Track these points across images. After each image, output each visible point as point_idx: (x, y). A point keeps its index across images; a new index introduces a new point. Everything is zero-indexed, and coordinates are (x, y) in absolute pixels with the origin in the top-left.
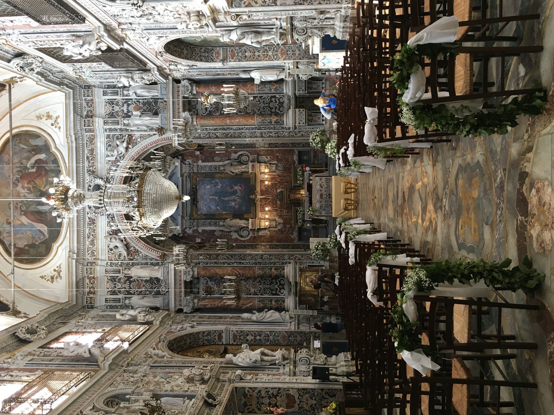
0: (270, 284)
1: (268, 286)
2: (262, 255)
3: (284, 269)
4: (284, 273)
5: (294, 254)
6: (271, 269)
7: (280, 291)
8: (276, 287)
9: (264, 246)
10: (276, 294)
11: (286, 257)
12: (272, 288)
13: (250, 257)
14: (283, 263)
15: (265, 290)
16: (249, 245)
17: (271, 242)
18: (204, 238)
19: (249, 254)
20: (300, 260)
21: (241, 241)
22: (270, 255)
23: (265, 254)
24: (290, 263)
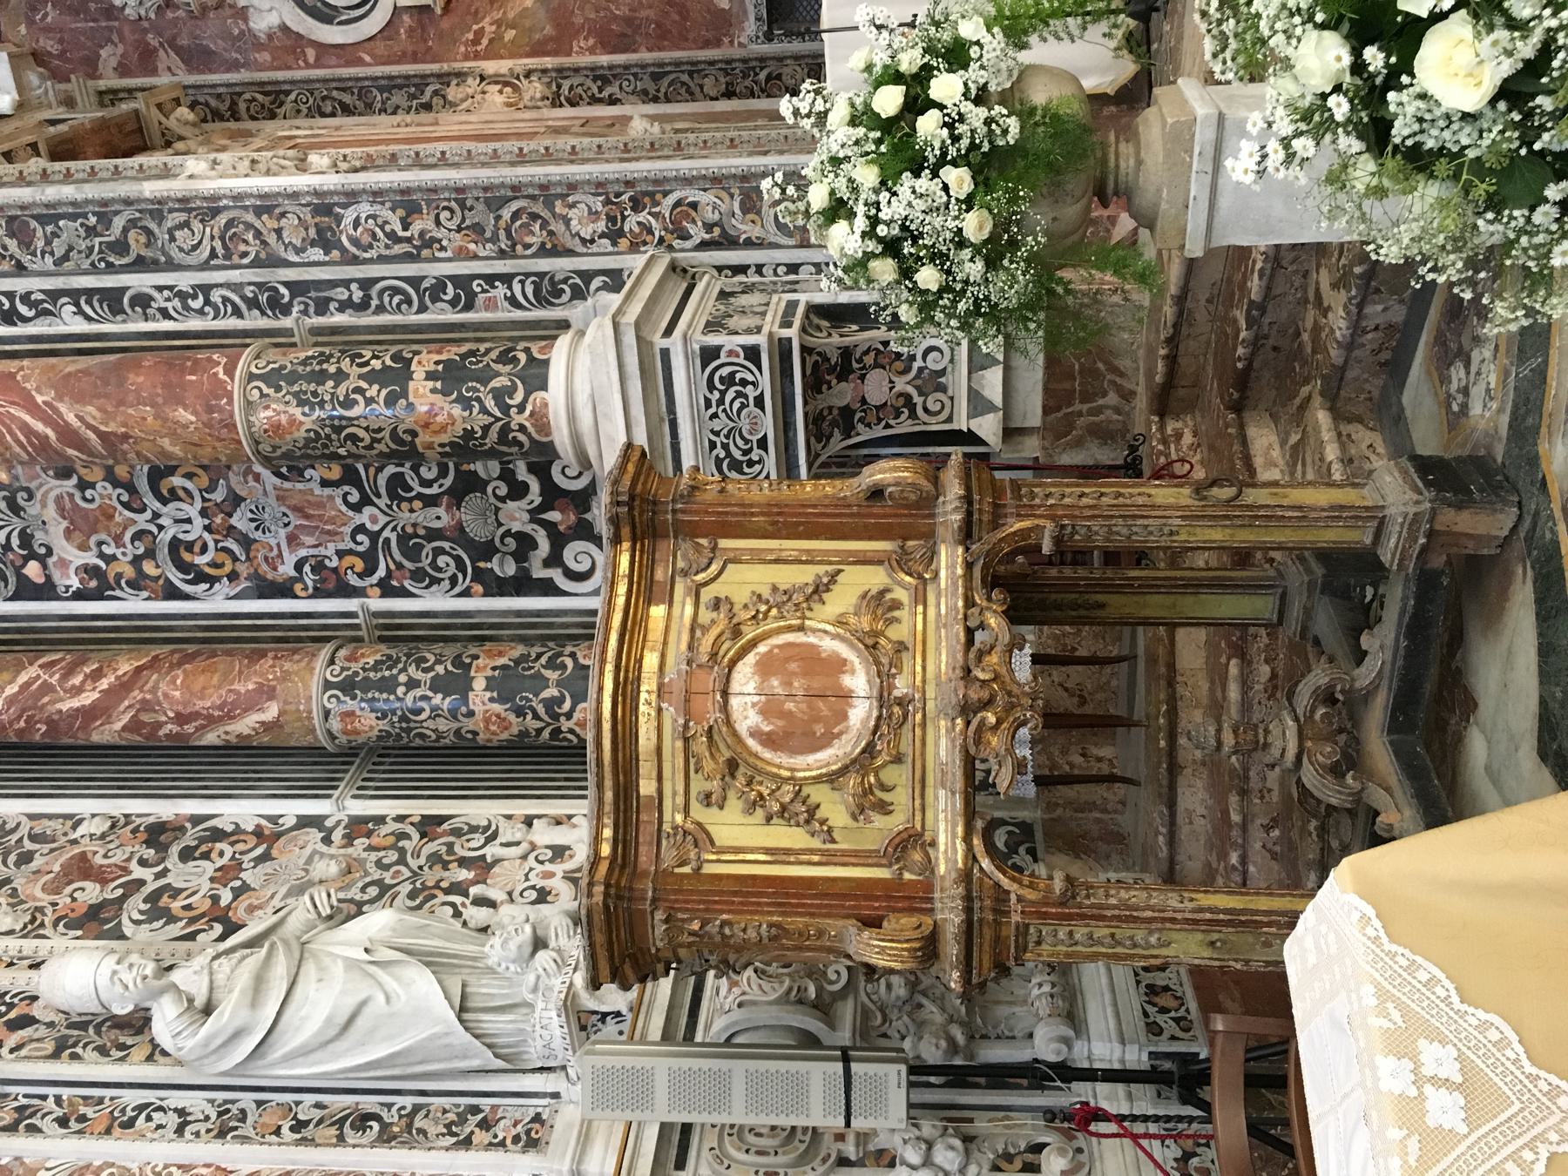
0: (457, 495)
1: (441, 517)
2: (325, 207)
3: (536, 375)
4: (541, 419)
5: (661, 185)
6: (396, 378)
7: (554, 560)
8: (516, 516)
9: (503, 82)
10: (522, 585)
11: (582, 219)
12: (478, 530)
13: (205, 235)
14: (547, 290)
15: (413, 553)
16: (391, 85)
17: (557, 45)
18: (49, 45)
19: (184, 202)
20: (728, 241)
21: (323, 49)
22: (408, 203)
23: (352, 197)
24: (615, 280)
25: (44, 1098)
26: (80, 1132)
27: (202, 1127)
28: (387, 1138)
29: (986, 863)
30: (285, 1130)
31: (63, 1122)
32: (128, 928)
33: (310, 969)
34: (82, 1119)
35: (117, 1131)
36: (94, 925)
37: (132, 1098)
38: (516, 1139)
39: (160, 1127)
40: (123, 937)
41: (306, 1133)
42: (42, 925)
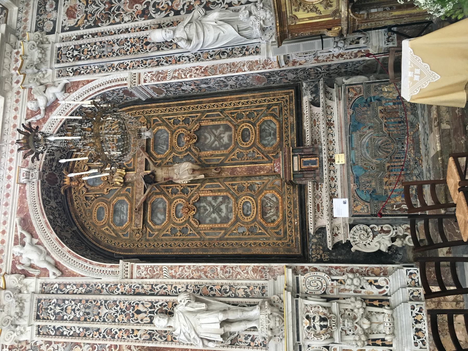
25: (160, 58)
26: (171, 64)
27: (193, 59)
28: (229, 56)
29: (351, 15)
30: (209, 57)
31: (167, 62)
32: (154, 16)
33: (205, 28)
34: (170, 61)
35: (178, 62)
36: (145, 16)
37: (177, 55)
38: (254, 52)
39: (185, 60)
40: (153, 18)
41: (214, 57)
42: (134, 18)
